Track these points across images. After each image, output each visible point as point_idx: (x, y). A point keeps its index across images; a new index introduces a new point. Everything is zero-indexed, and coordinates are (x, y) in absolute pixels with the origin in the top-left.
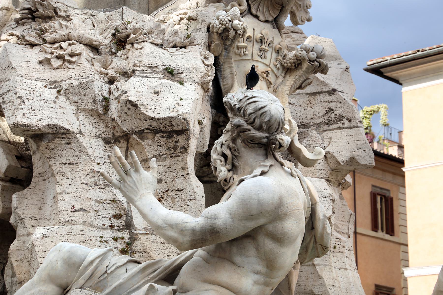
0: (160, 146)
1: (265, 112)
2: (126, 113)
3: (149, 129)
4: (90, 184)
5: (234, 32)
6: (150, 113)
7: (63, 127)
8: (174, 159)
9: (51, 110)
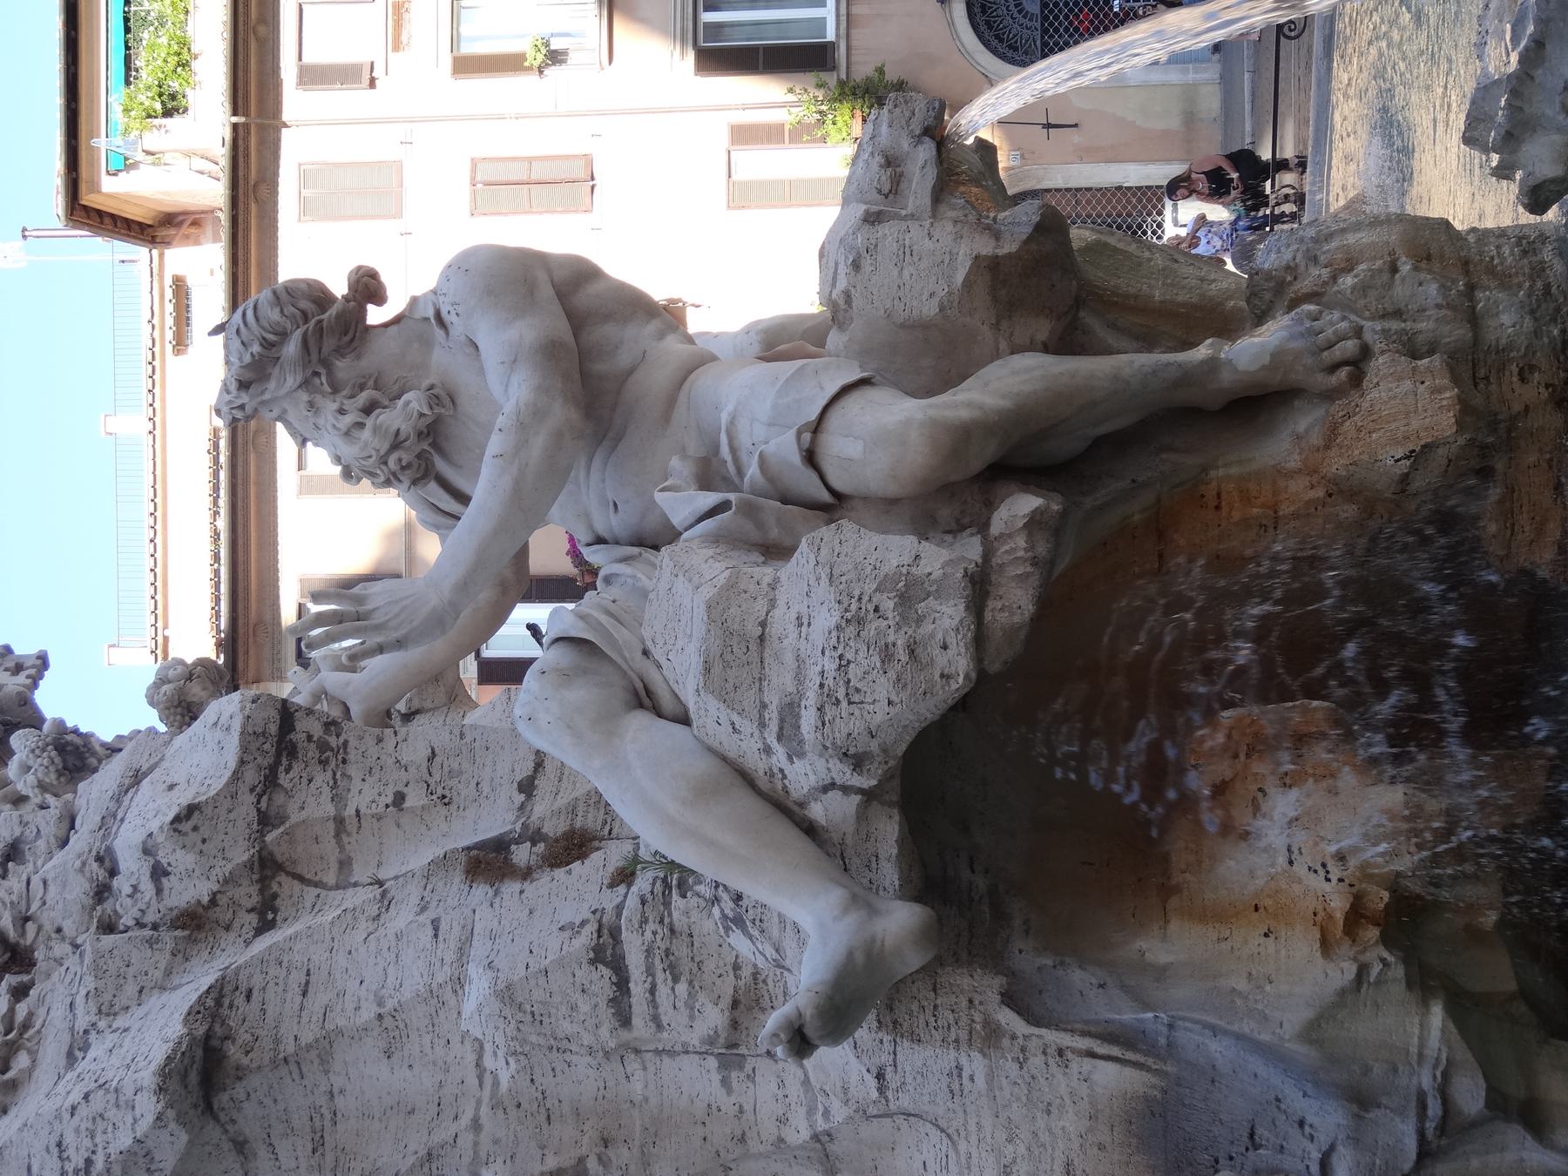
0: (310, 781)
2: (204, 841)
3: (260, 796)
7: (200, 997)
8: (352, 757)
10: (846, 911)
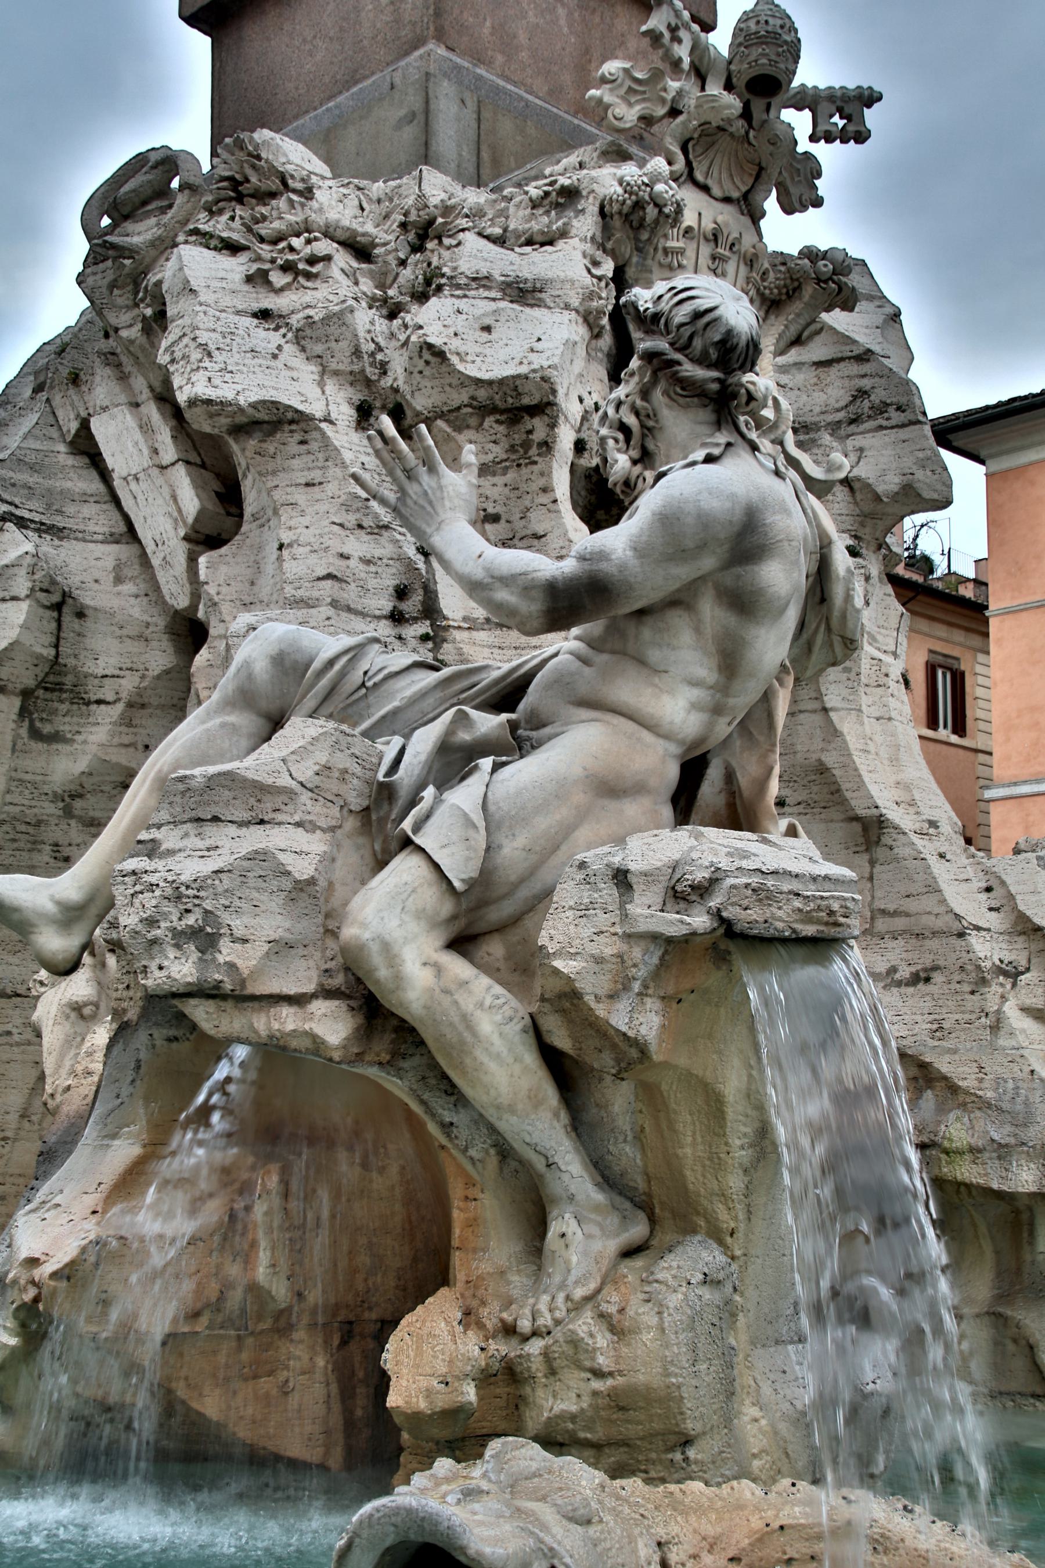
0: (495, 442)
2: (421, 372)
3: (470, 406)
4: (347, 524)
5: (656, 211)
6: (471, 370)
7: (290, 407)
8: (524, 471)
9: (267, 371)
10: (58, 903)
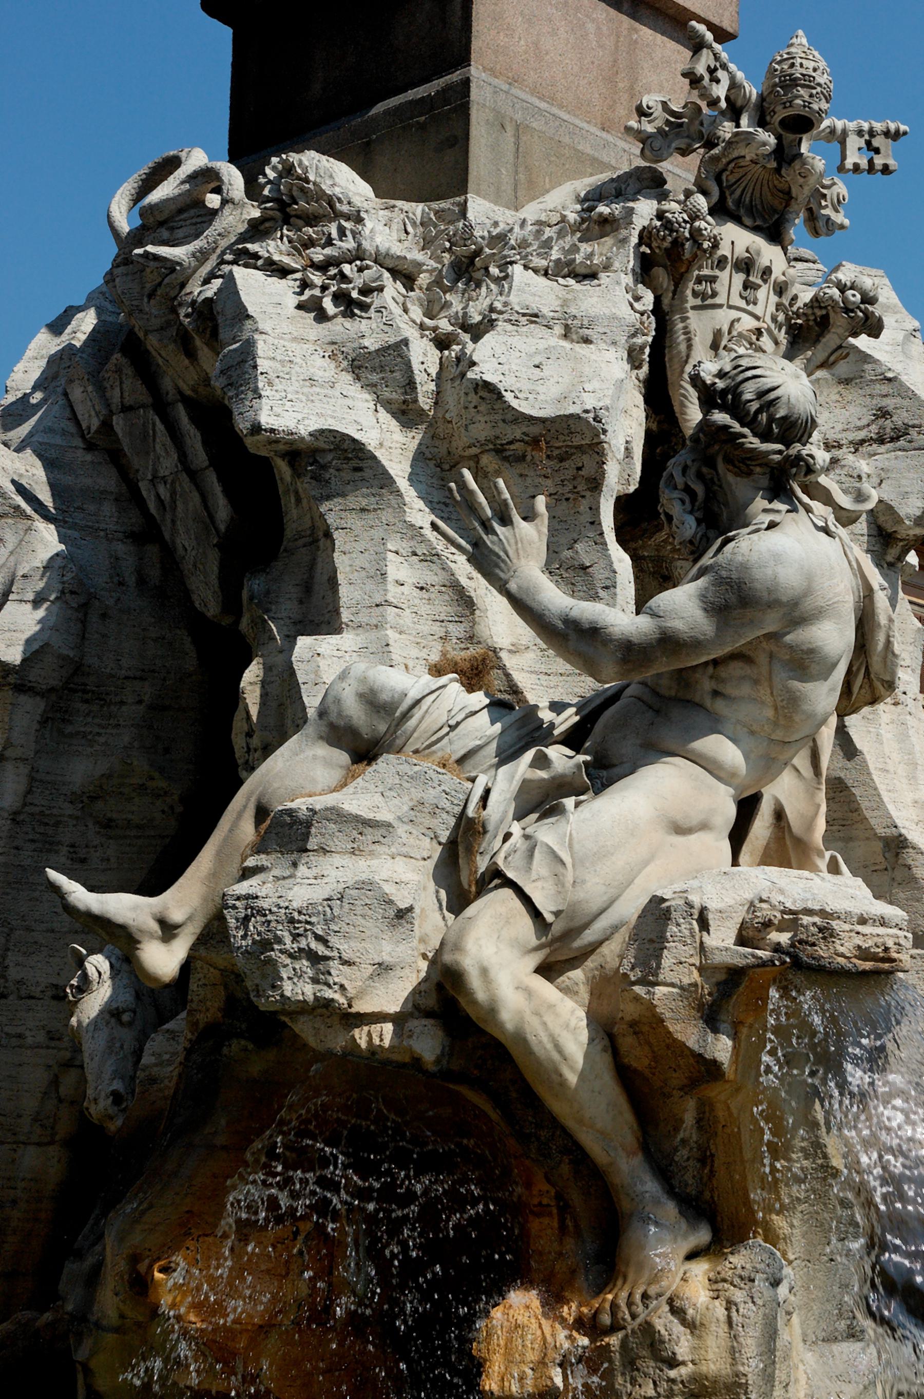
1: (778, 398)
4: (401, 551)
9: (325, 400)
